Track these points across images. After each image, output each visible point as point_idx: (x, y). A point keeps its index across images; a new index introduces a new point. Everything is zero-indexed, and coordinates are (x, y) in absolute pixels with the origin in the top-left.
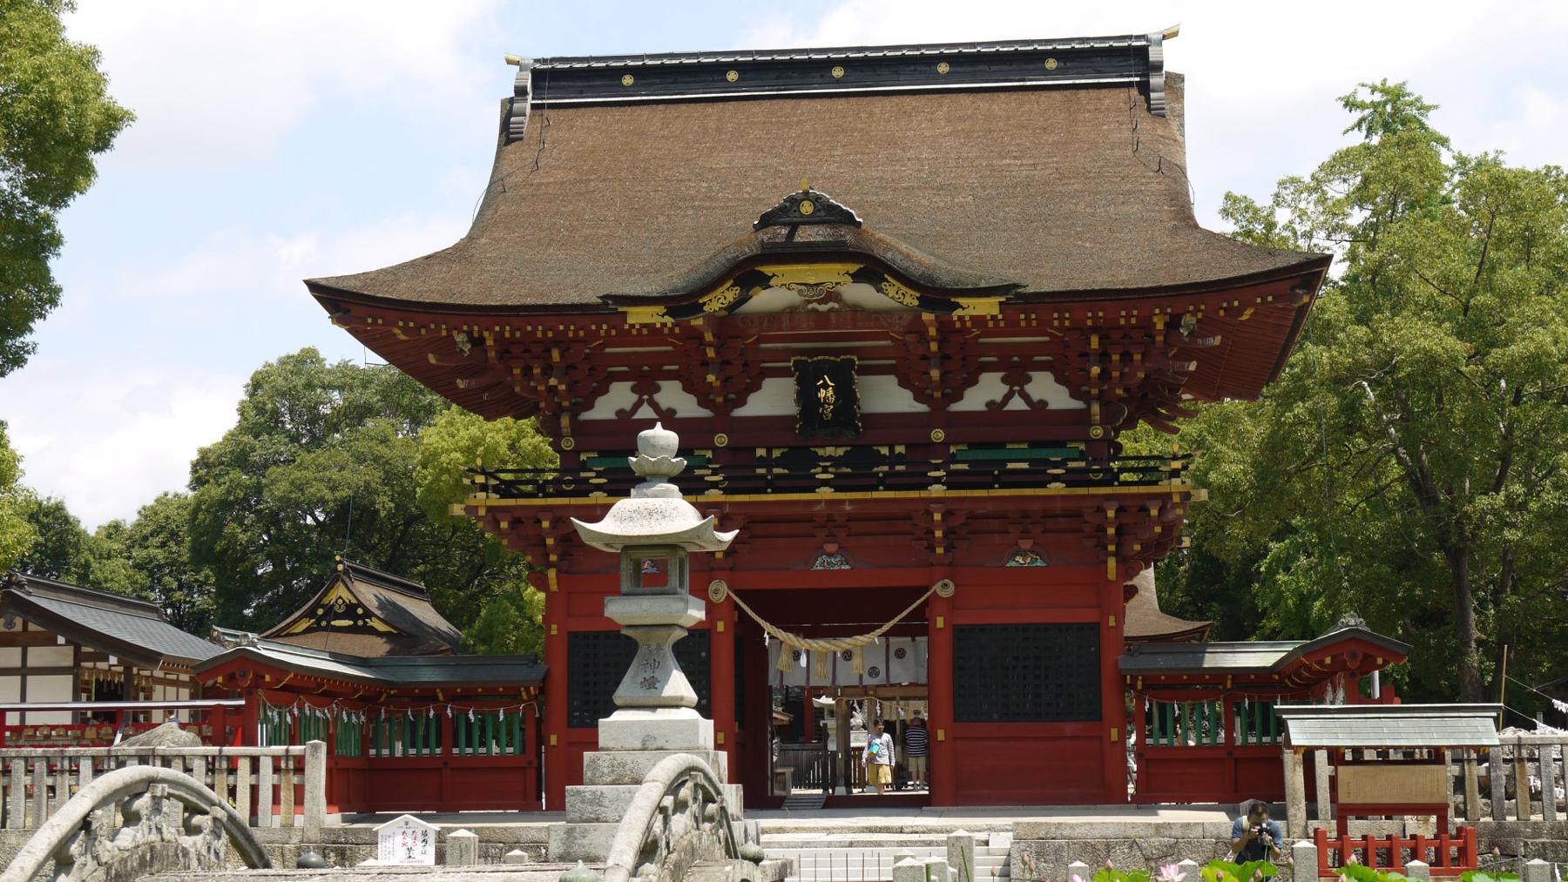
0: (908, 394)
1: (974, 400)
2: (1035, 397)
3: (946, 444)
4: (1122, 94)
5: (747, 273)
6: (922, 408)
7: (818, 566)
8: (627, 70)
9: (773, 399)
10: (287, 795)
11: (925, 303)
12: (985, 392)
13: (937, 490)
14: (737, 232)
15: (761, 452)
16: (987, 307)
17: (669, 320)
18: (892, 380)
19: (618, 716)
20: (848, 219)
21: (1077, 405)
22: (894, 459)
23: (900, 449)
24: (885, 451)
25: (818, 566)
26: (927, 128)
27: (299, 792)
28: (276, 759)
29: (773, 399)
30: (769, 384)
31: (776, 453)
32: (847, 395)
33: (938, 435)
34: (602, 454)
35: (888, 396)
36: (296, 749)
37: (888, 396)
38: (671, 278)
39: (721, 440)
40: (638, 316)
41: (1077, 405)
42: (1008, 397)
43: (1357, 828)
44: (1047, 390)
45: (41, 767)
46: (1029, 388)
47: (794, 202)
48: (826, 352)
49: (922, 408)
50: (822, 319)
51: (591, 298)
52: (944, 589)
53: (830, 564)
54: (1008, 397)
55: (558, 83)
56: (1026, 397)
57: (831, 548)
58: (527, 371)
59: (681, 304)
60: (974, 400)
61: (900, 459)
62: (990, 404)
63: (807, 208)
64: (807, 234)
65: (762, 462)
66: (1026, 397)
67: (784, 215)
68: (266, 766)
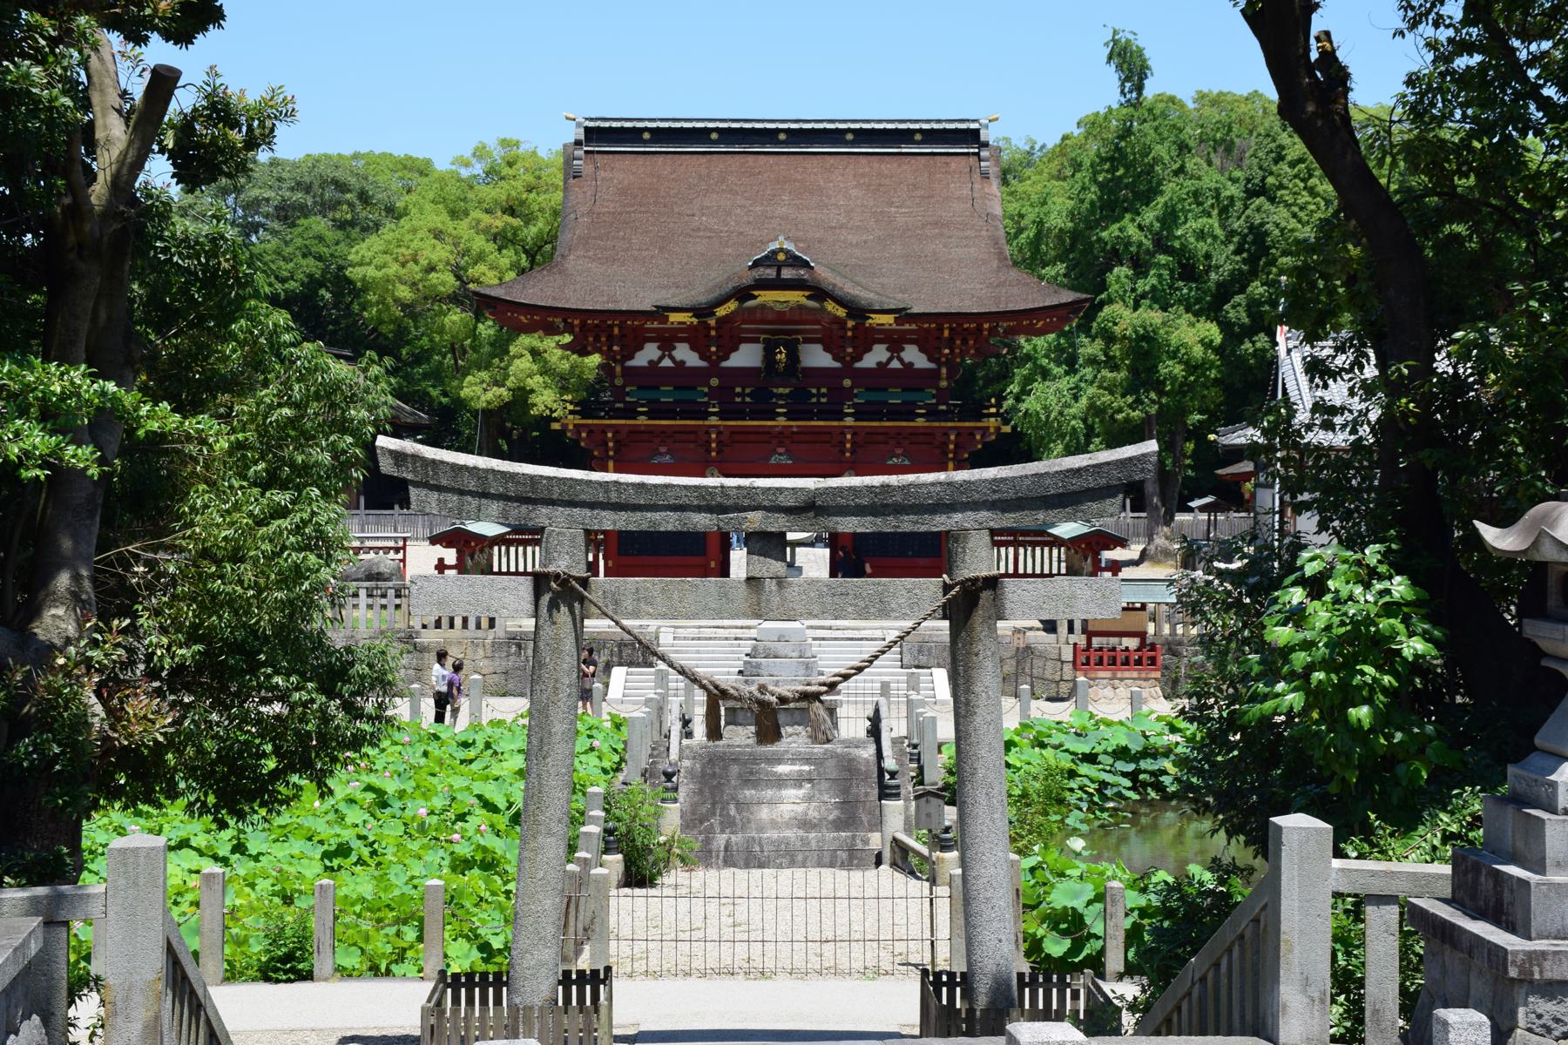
0: (829, 356)
1: (870, 360)
2: (907, 360)
3: (852, 388)
5: (743, 294)
6: (837, 365)
7: (773, 461)
9: (746, 356)
11: (849, 315)
12: (876, 356)
13: (849, 421)
14: (739, 270)
15: (738, 390)
16: (888, 320)
17: (695, 320)
18: (818, 348)
20: (806, 264)
21: (932, 366)
23: (824, 390)
24: (814, 391)
25: (773, 461)
26: (844, 182)
29: (746, 356)
30: (744, 347)
31: (748, 391)
32: (793, 356)
33: (847, 383)
35: (817, 357)
37: (817, 357)
38: (700, 295)
39: (714, 382)
40: (675, 318)
41: (932, 366)
42: (890, 360)
43: (1096, 641)
44: (914, 356)
46: (903, 355)
47: (775, 253)
48: (782, 333)
49: (837, 365)
51: (647, 305)
54: (890, 360)
55: (598, 135)
56: (901, 360)
57: (781, 450)
60: (870, 360)
61: (824, 395)
62: (879, 364)
63: (781, 257)
65: (738, 395)
66: (901, 360)
67: (770, 260)
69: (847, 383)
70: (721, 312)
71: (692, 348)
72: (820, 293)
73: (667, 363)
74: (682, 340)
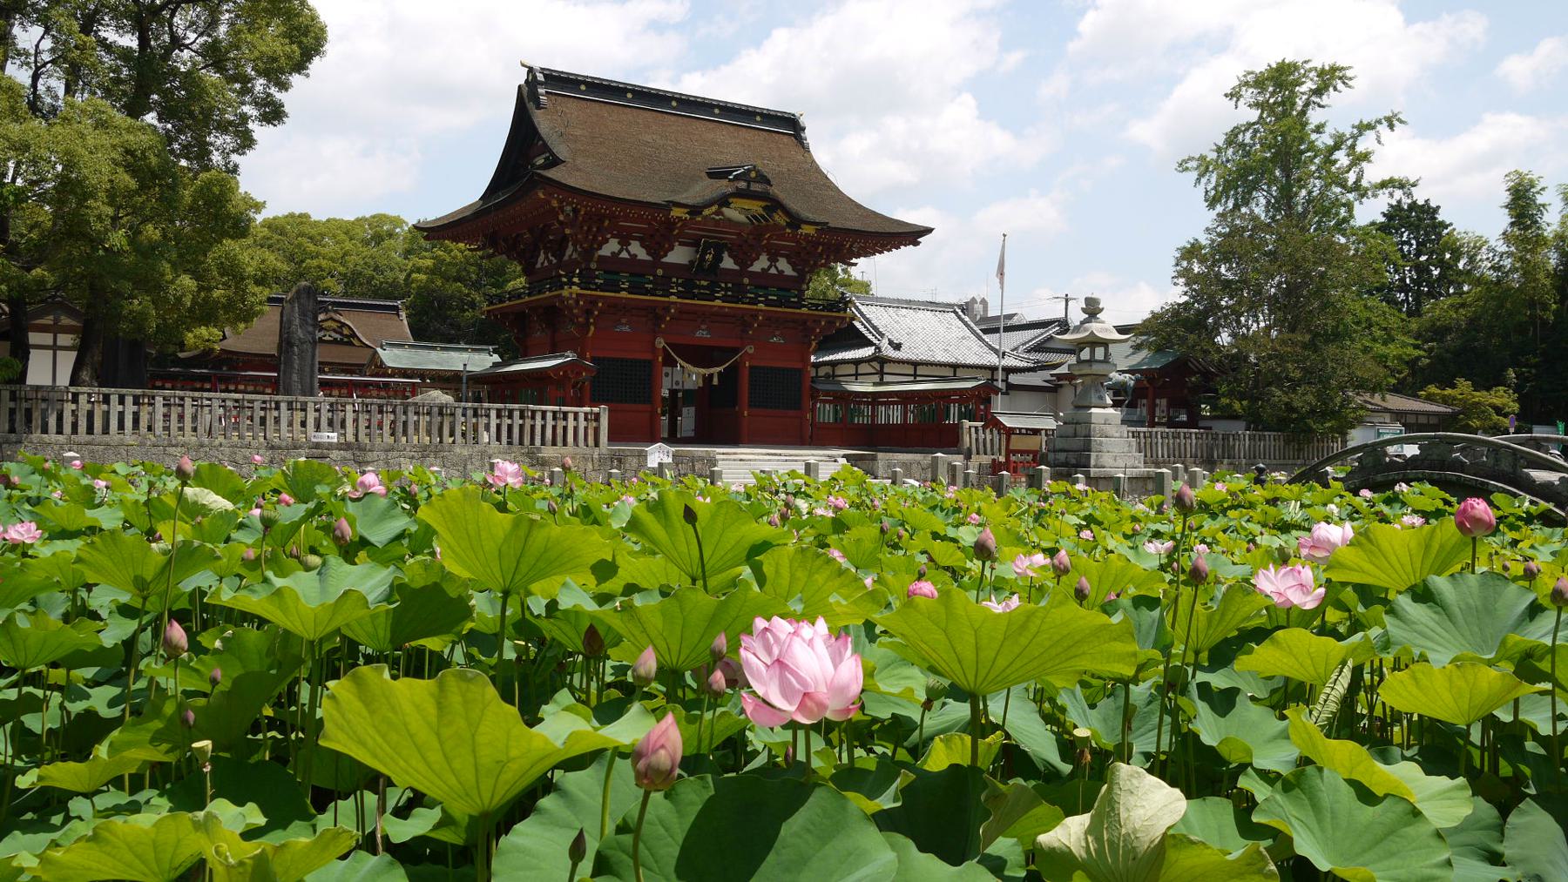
1: (757, 267)
4: (785, 139)
8: (584, 82)
9: (679, 255)
10: (591, 432)
12: (761, 264)
19: (1093, 410)
20: (768, 182)
22: (727, 289)
27: (597, 430)
28: (554, 413)
29: (679, 255)
32: (718, 259)
34: (632, 275)
35: (728, 263)
36: (596, 410)
37: (728, 263)
40: (677, 212)
43: (1013, 458)
45: (470, 413)
50: (717, 223)
52: (750, 350)
53: (702, 334)
58: (590, 229)
59: (695, 210)
60: (757, 267)
63: (753, 174)
64: (756, 187)
68: (549, 416)
69: (746, 281)
70: (706, 212)
71: (642, 246)
72: (774, 205)
73: (624, 255)
74: (635, 239)
